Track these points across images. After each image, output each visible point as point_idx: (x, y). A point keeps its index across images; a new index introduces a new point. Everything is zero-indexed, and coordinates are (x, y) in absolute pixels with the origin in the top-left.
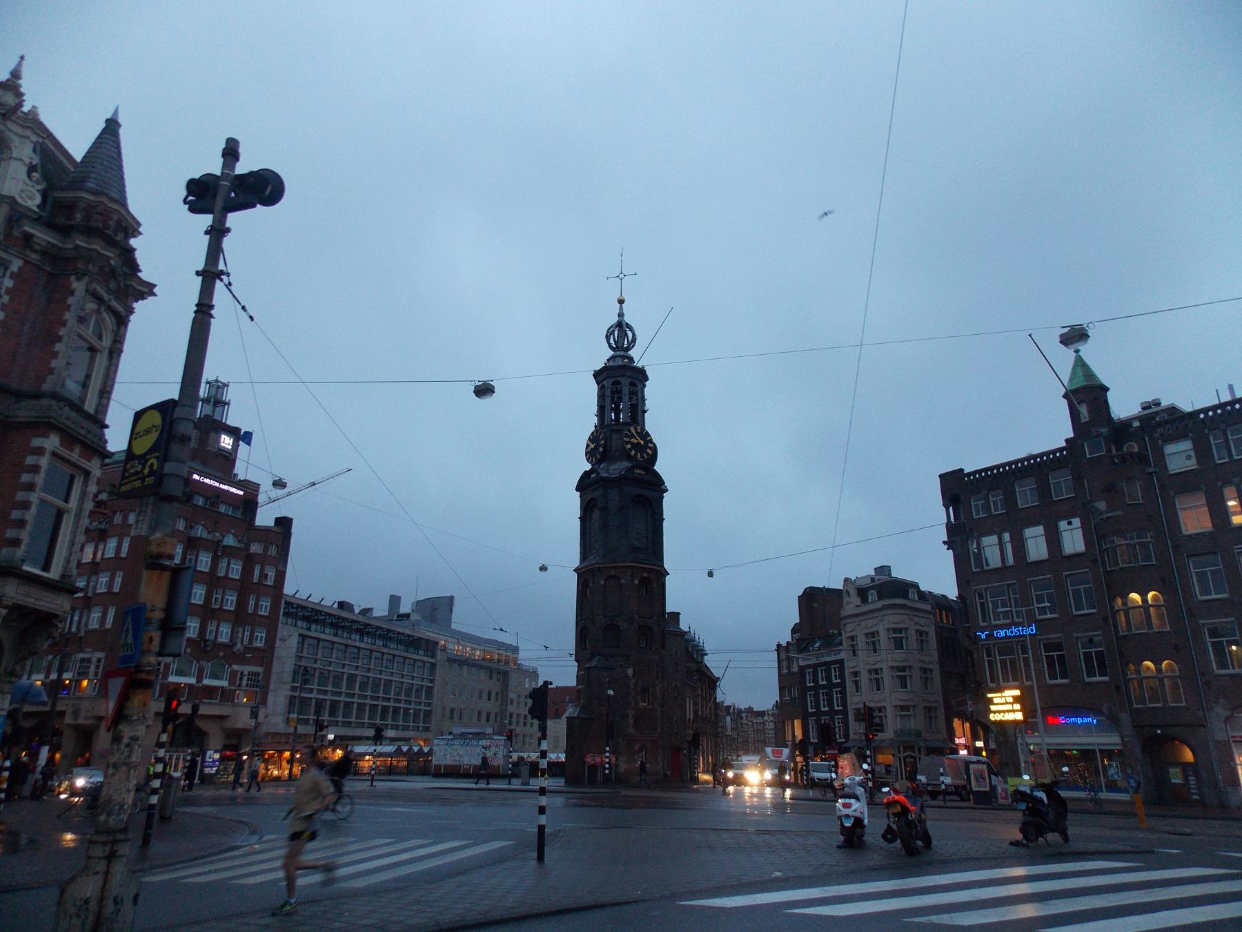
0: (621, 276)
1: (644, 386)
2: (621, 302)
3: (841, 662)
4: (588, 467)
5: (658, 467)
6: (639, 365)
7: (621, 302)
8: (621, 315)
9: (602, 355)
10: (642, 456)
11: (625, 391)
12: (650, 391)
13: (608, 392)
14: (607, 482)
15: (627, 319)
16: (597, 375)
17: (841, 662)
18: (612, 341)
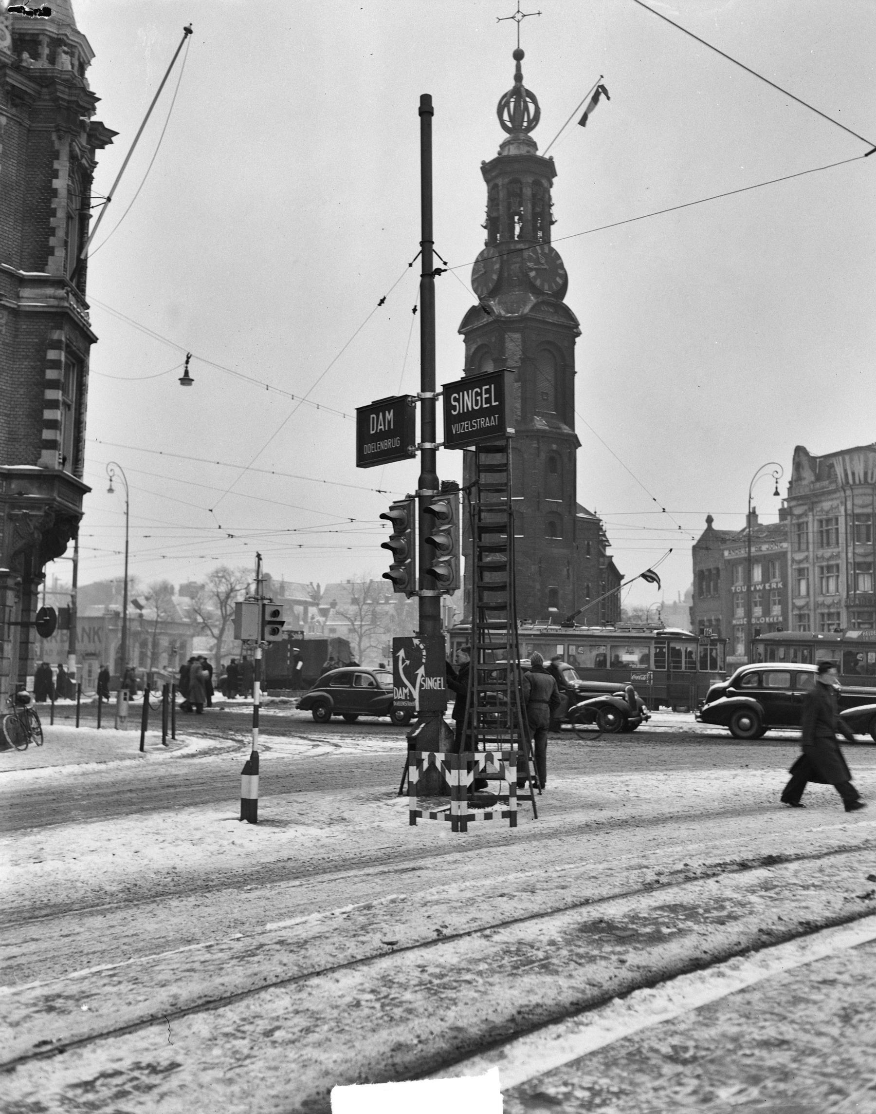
0: (519, 16)
1: (551, 185)
2: (519, 55)
3: (785, 554)
4: (474, 300)
5: (568, 300)
6: (547, 156)
7: (519, 55)
8: (518, 77)
9: (491, 140)
10: (550, 288)
11: (528, 192)
12: (558, 191)
13: (502, 195)
14: (502, 325)
15: (527, 84)
16: (489, 170)
17: (785, 554)
18: (506, 117)
